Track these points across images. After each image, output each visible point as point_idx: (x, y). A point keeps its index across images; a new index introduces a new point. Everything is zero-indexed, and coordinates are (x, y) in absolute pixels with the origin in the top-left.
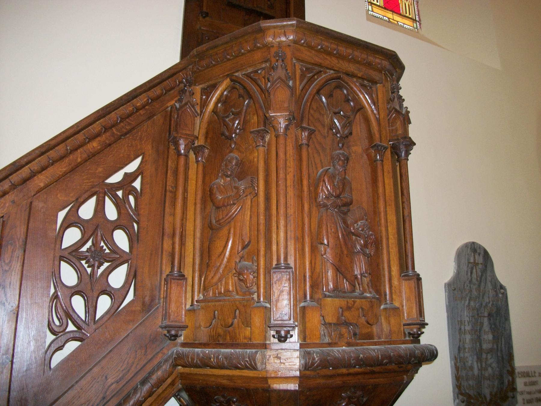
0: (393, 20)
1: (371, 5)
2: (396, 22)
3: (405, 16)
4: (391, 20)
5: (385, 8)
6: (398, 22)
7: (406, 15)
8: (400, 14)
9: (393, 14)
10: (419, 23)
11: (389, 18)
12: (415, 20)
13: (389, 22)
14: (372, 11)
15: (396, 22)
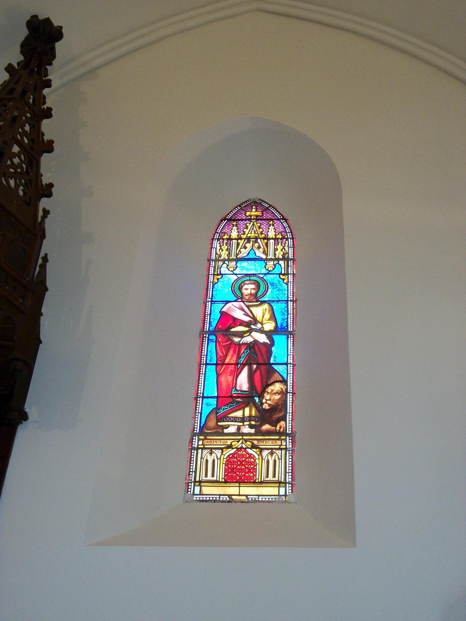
0: (239, 495)
1: (200, 485)
2: (244, 498)
3: (262, 482)
4: (233, 497)
5: (226, 482)
6: (246, 496)
7: (267, 479)
8: (254, 482)
9: (239, 487)
10: (292, 484)
11: (230, 496)
12: (285, 483)
13: (231, 501)
14: (200, 494)
15: (244, 498)
